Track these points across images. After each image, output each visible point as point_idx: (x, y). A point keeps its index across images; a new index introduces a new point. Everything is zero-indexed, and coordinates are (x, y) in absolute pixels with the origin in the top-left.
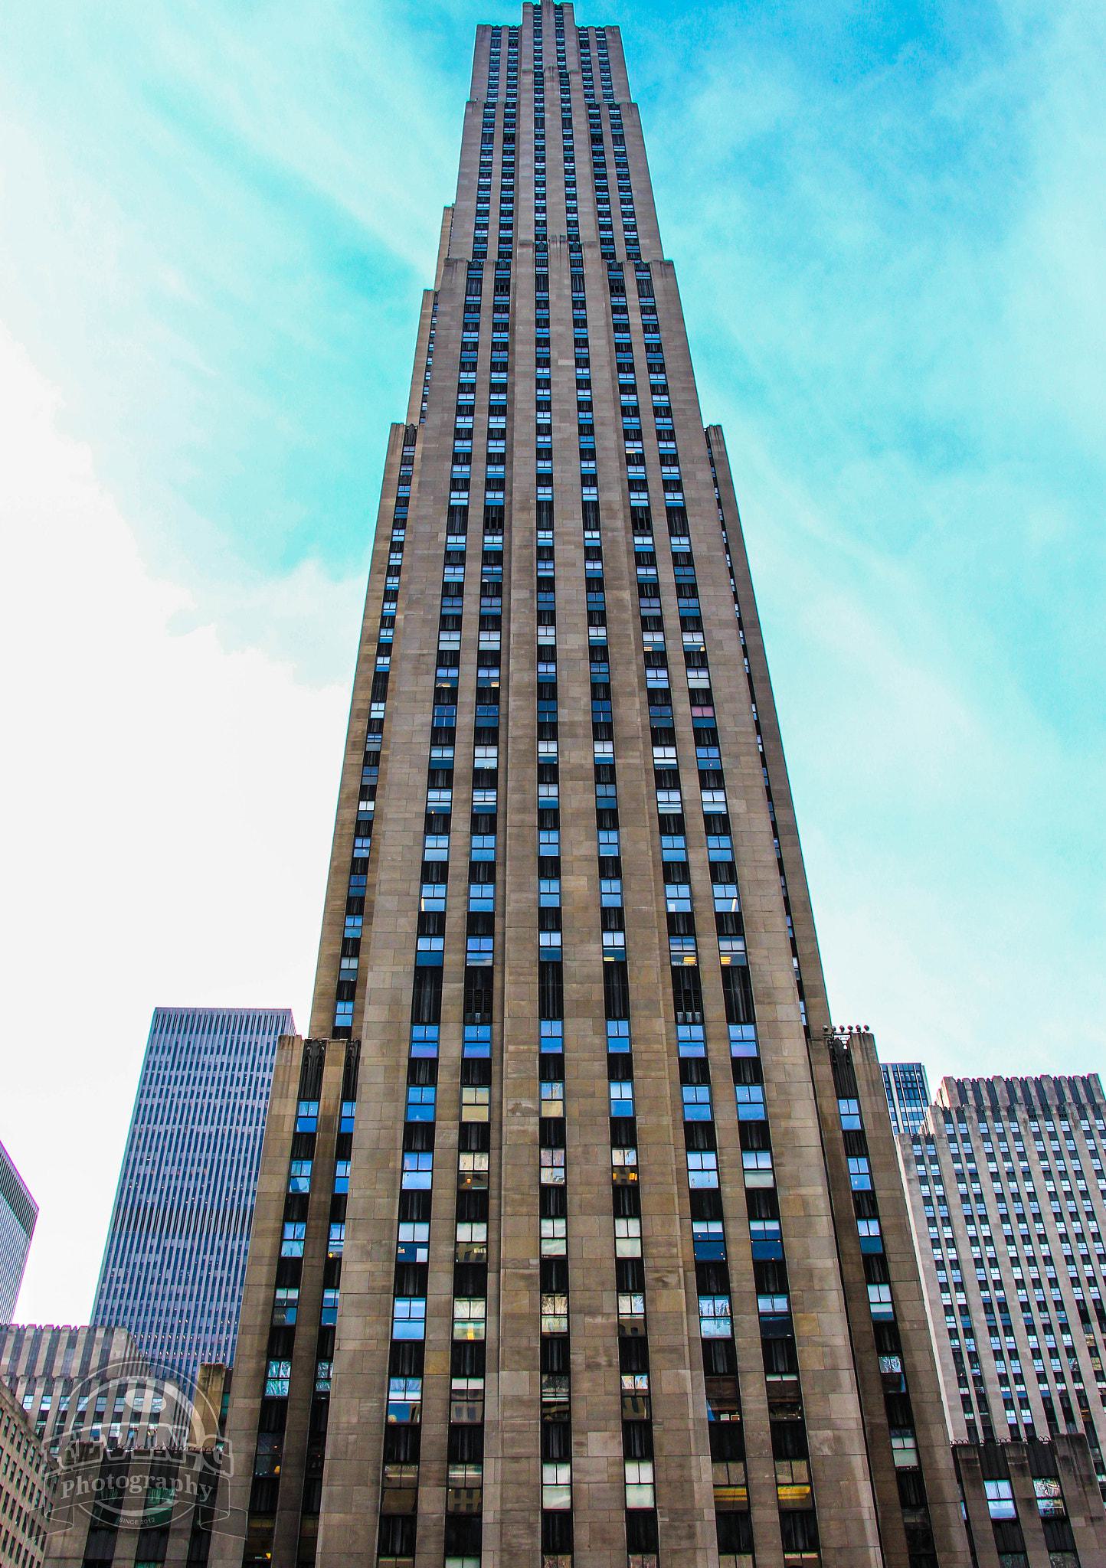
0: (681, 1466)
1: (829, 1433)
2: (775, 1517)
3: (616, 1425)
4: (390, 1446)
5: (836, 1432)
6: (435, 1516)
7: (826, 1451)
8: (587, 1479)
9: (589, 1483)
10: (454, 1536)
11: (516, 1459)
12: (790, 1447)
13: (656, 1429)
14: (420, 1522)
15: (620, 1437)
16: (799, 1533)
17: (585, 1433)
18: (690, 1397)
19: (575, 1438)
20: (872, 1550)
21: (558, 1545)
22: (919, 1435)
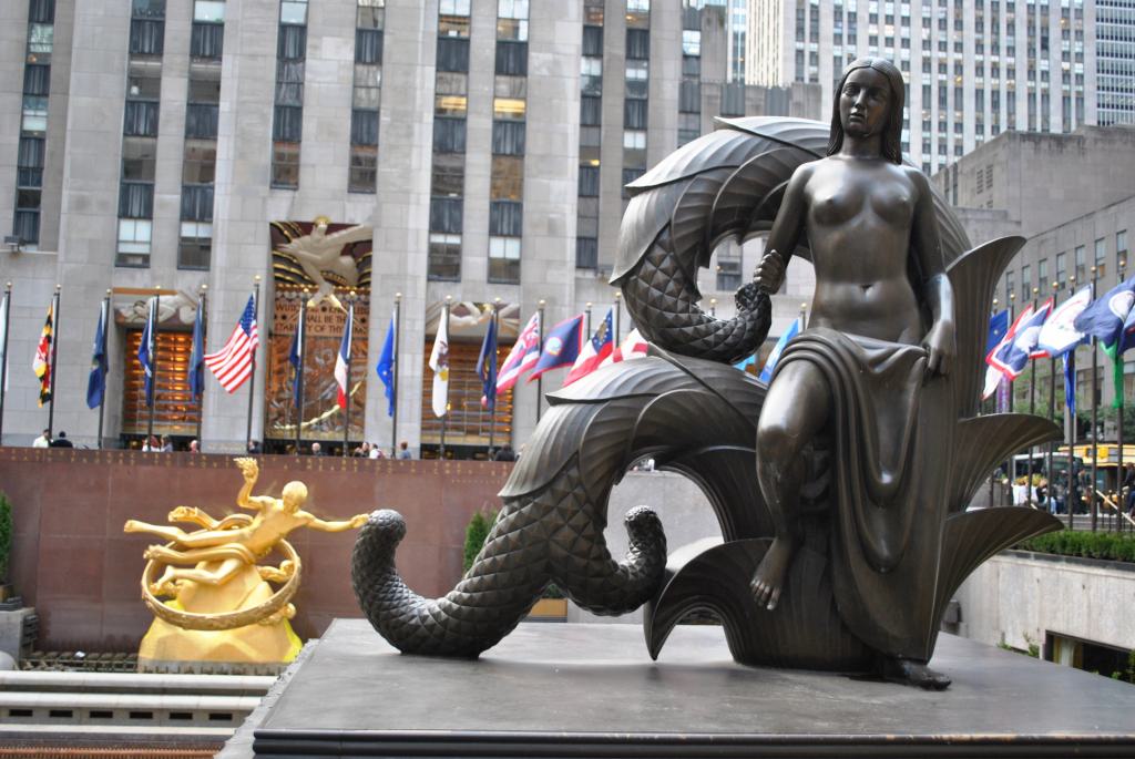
0: (407, 74)
1: (549, 57)
2: (489, 125)
3: (352, 33)
4: (134, 38)
5: (557, 56)
6: (176, 104)
7: (545, 72)
8: (318, 79)
9: (319, 83)
10: (193, 122)
11: (253, 56)
12: (511, 65)
13: (387, 39)
14: (163, 108)
15: (352, 43)
16: (508, 140)
17: (319, 37)
18: (422, 12)
19: (310, 41)
20: (570, 160)
21: (287, 135)
22: (653, 67)
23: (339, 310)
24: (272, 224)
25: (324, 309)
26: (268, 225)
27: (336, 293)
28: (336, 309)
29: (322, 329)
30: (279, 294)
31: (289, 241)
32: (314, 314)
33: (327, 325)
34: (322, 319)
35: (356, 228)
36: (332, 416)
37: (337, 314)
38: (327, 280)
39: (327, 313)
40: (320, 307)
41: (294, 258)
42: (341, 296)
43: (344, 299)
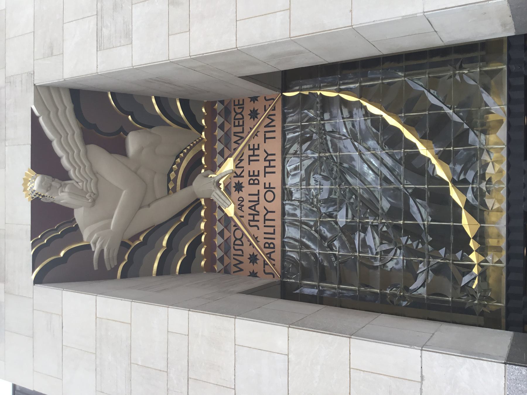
23: (239, 161)
24: (38, 281)
25: (239, 187)
26: (38, 287)
27: (213, 167)
28: (236, 167)
29: (269, 188)
30: (218, 267)
31: (88, 247)
32: (246, 204)
33: (261, 178)
34: (254, 189)
35: (41, 120)
36: (444, 157)
37: (245, 163)
38: (187, 181)
39: (244, 181)
40: (235, 195)
41: (136, 237)
42: (218, 159)
43: (222, 153)
